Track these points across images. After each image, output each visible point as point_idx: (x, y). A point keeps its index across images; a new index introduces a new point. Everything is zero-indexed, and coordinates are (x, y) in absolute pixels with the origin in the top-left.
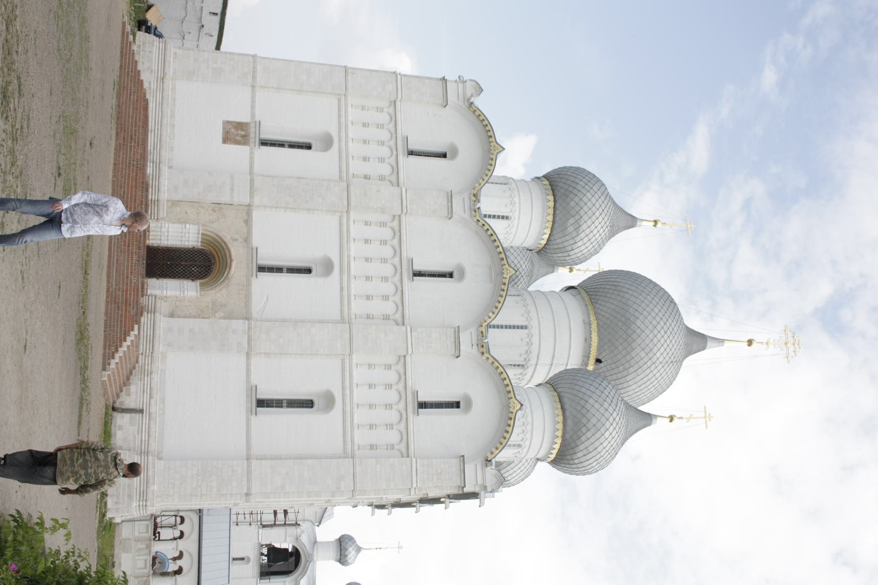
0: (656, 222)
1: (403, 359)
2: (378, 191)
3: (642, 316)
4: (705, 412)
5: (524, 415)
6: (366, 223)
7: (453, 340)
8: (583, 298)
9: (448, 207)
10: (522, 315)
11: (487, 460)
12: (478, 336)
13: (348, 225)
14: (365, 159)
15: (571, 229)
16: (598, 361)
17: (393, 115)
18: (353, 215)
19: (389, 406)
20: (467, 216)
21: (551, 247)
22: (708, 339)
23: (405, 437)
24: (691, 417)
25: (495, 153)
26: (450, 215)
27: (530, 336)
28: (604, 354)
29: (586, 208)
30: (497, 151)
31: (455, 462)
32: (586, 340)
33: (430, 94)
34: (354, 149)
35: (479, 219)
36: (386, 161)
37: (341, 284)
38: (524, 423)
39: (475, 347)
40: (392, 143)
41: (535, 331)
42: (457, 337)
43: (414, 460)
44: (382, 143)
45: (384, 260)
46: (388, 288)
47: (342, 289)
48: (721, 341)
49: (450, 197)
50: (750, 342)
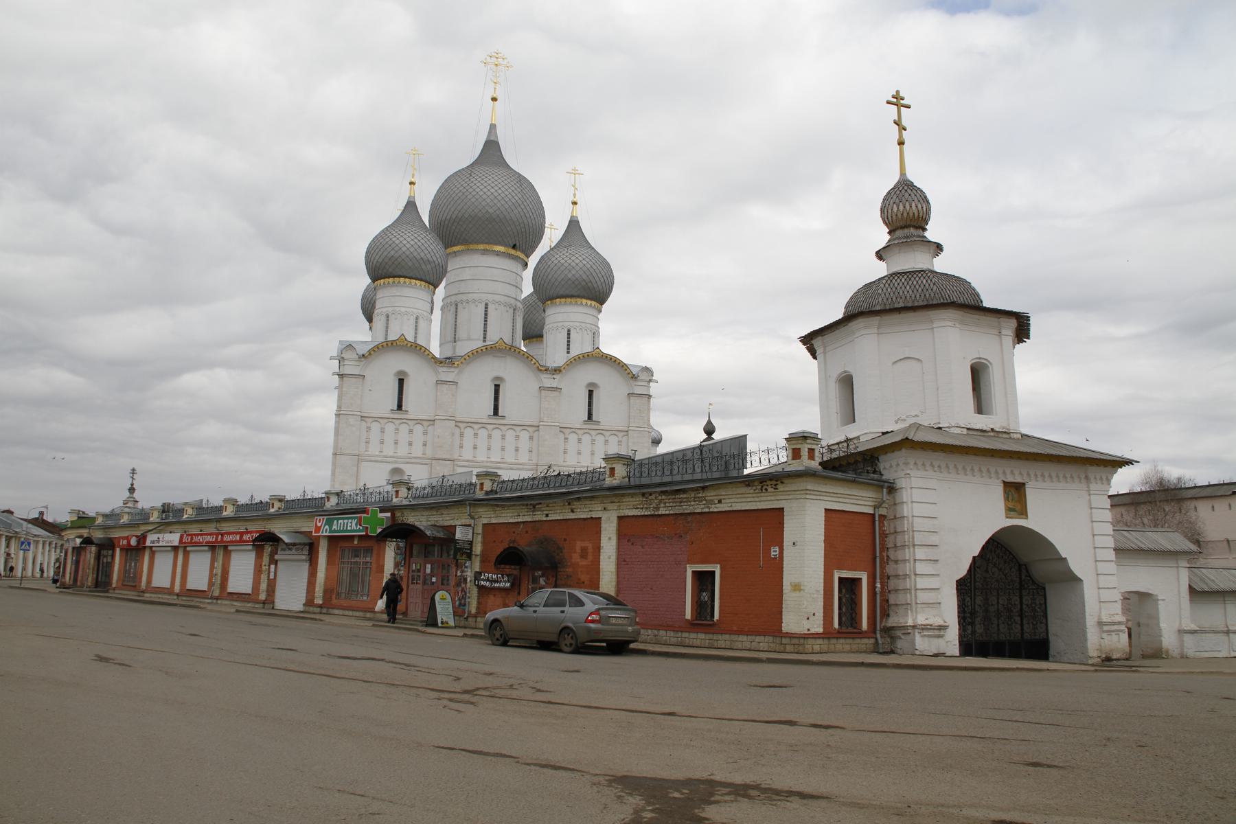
0: (412, 183)
1: (562, 429)
2: (438, 437)
3: (479, 200)
4: (571, 173)
6: (461, 447)
8: (460, 252)
10: (477, 306)
11: (632, 378)
13: (463, 461)
14: (410, 444)
15: (429, 267)
16: (514, 247)
17: (374, 419)
18: (456, 457)
19: (593, 442)
20: (456, 371)
21: (432, 279)
23: (614, 432)
24: (574, 186)
27: (494, 302)
28: (510, 242)
29: (415, 254)
31: (633, 399)
32: (498, 255)
34: (403, 451)
36: (411, 428)
37: (507, 469)
39: (555, 376)
40: (397, 422)
41: (490, 297)
43: (630, 428)
44: (397, 430)
45: (490, 436)
46: (510, 435)
47: (511, 469)
48: (493, 127)
49: (440, 382)
50: (494, 99)
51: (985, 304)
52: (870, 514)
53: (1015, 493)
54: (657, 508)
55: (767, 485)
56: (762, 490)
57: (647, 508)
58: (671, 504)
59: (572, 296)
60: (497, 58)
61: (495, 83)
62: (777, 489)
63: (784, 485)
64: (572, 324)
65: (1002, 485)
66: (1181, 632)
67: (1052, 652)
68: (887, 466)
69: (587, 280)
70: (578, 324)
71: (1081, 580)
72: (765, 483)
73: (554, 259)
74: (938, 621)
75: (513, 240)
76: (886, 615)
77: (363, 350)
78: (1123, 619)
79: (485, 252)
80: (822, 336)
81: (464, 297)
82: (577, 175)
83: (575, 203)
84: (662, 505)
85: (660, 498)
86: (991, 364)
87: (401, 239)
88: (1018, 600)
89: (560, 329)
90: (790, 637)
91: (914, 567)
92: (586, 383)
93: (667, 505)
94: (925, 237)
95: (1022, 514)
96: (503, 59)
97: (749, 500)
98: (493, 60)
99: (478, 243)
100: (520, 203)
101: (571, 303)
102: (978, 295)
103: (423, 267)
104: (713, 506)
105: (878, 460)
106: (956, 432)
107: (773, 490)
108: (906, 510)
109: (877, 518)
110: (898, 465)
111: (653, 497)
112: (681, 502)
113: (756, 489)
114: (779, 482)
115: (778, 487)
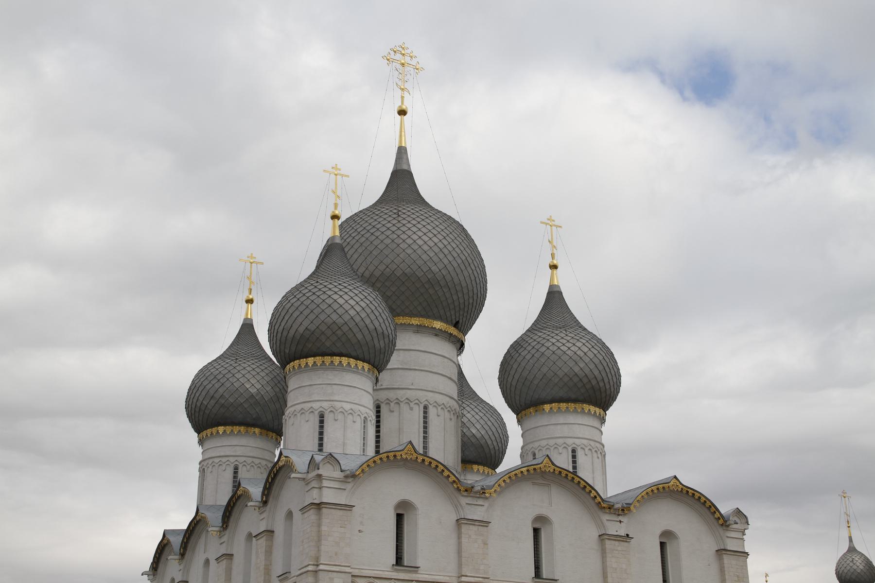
3: (401, 256)
5: (581, 448)
7: (617, 543)
9: (479, 525)
10: (411, 409)
11: (722, 525)
12: (610, 513)
16: (456, 325)
20: (486, 504)
22: (399, 168)
25: (415, 455)
26: (485, 523)
27: (437, 405)
28: (453, 317)
30: (413, 452)
32: (436, 335)
33: (341, 527)
35: (493, 490)
38: (590, 449)
39: (620, 518)
42: (615, 538)
48: (402, 152)
50: (402, 113)
59: (575, 401)
60: (403, 55)
61: (402, 90)
64: (577, 441)
69: (599, 378)
70: (585, 442)
73: (529, 348)
75: (457, 315)
77: (350, 465)
79: (420, 329)
81: (392, 395)
82: (553, 227)
83: (554, 267)
87: (346, 297)
89: (560, 449)
92: (659, 532)
96: (411, 57)
98: (398, 56)
99: (411, 315)
100: (470, 261)
101: (575, 411)
103: (376, 341)
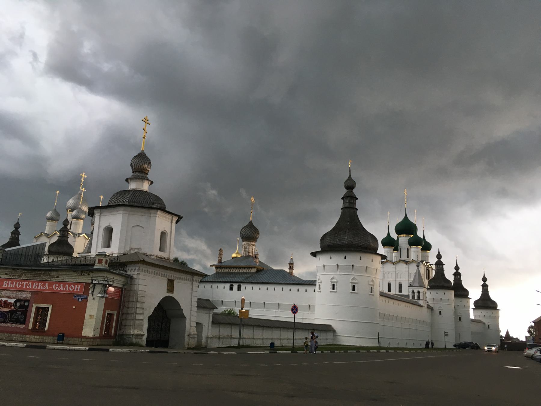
51: (167, 209)
52: (121, 288)
53: (171, 284)
54: (20, 276)
55: (85, 273)
56: (81, 274)
57: (13, 275)
58: (29, 275)
62: (89, 275)
63: (93, 273)
65: (167, 280)
66: (207, 338)
67: (169, 345)
68: (130, 269)
71: (186, 318)
72: (84, 272)
74: (142, 333)
76: (120, 329)
78: (195, 332)
80: (101, 209)
84: (24, 275)
85: (23, 271)
86: (167, 233)
88: (161, 324)
90: (86, 338)
91: (136, 310)
93: (27, 275)
94: (147, 178)
95: (172, 292)
97: (73, 278)
102: (165, 205)
104: (53, 278)
105: (126, 267)
106: (153, 258)
107: (87, 275)
108: (136, 288)
109: (124, 290)
110: (135, 269)
111: (19, 271)
112: (35, 275)
113: (79, 274)
114: (91, 272)
115: (90, 274)
